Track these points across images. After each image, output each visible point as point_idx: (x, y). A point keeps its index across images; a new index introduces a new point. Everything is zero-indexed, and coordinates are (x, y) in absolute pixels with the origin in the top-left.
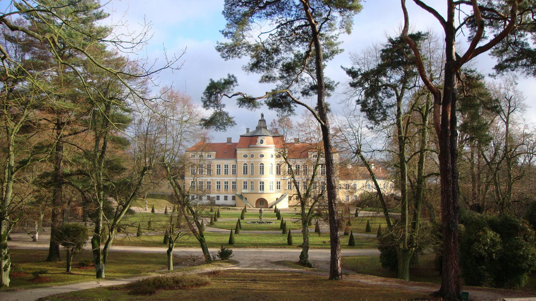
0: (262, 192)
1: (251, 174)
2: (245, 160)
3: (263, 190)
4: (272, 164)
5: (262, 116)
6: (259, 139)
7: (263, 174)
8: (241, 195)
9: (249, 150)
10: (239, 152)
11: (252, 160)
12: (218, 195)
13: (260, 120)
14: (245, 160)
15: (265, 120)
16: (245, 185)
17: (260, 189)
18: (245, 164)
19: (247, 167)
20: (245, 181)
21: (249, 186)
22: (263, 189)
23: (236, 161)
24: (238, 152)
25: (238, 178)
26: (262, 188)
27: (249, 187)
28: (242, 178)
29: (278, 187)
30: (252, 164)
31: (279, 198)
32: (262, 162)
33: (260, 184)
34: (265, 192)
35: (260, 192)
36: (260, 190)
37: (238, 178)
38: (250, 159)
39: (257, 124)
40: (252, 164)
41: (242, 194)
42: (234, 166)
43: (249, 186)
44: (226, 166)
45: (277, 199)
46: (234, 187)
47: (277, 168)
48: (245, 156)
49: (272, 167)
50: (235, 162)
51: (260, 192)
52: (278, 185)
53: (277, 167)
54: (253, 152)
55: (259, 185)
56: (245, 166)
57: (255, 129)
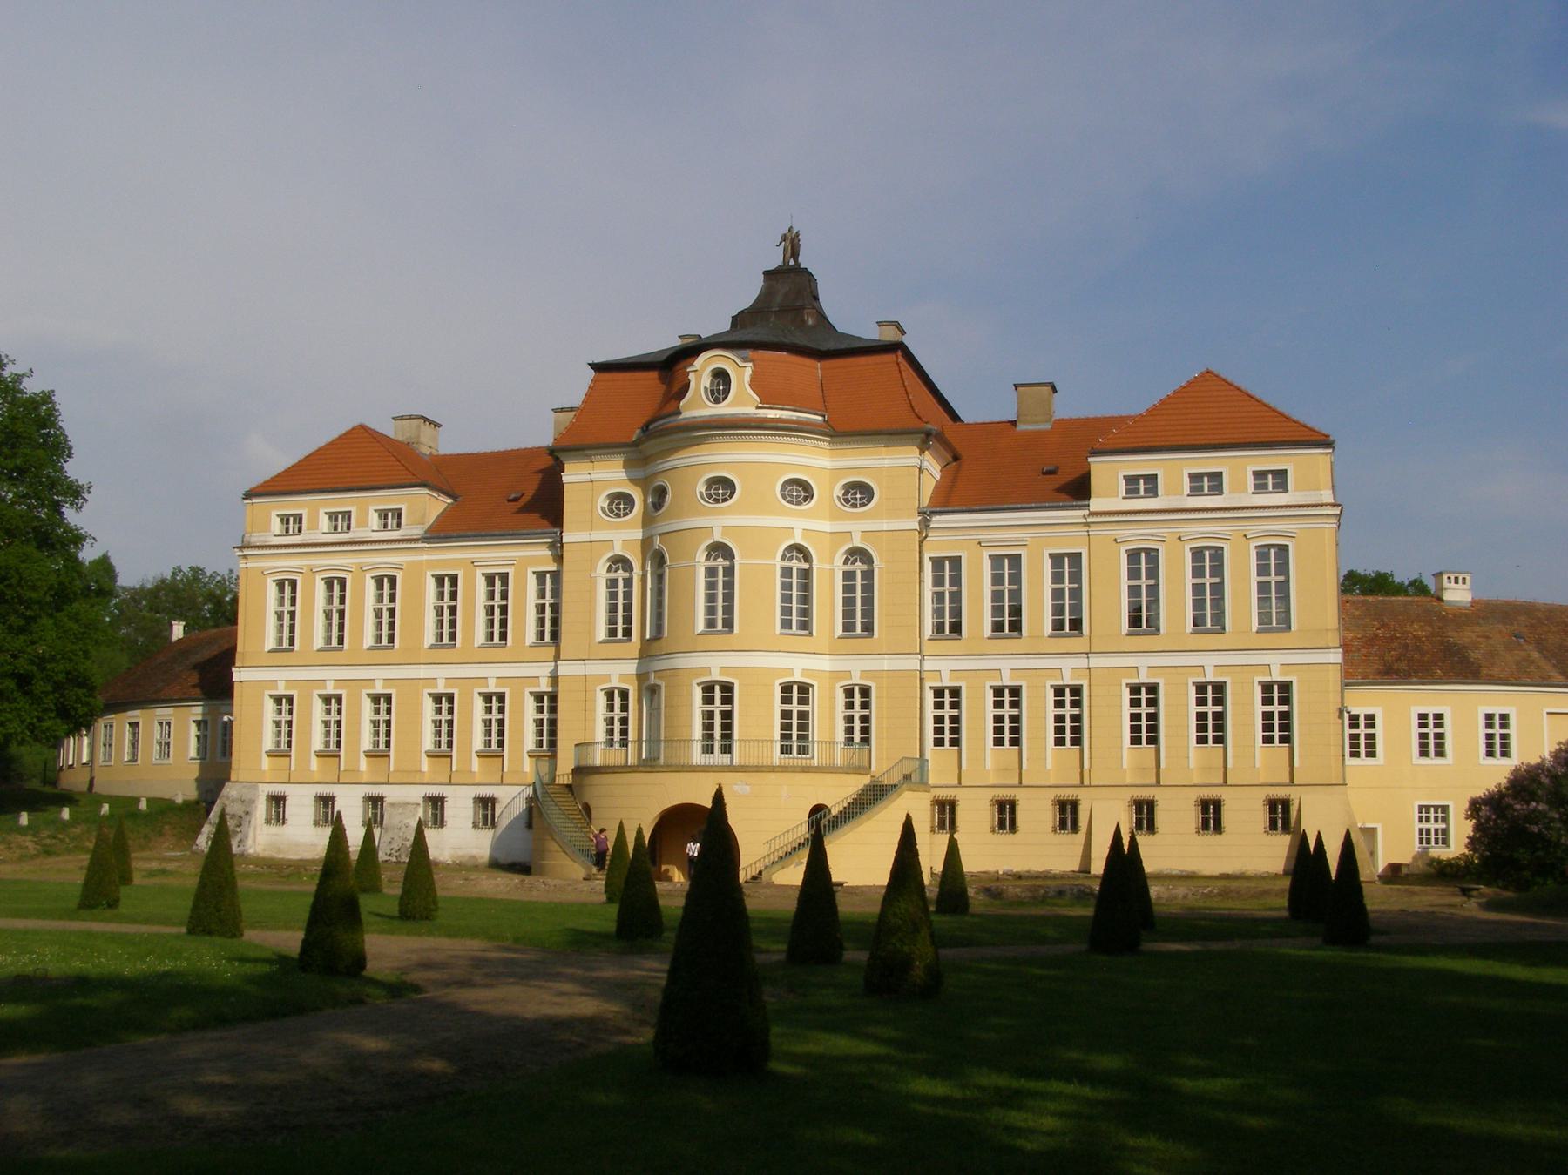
0: (718, 758)
3: (727, 749)
4: (800, 551)
5: (792, 244)
6: (701, 370)
10: (574, 475)
12: (434, 791)
17: (709, 737)
19: (628, 583)
20: (615, 683)
22: (727, 735)
24: (565, 478)
25: (564, 669)
34: (738, 756)
36: (709, 749)
37: (564, 669)
40: (659, 560)
42: (553, 581)
44: (497, 582)
48: (621, 503)
52: (857, 712)
57: (728, 327)
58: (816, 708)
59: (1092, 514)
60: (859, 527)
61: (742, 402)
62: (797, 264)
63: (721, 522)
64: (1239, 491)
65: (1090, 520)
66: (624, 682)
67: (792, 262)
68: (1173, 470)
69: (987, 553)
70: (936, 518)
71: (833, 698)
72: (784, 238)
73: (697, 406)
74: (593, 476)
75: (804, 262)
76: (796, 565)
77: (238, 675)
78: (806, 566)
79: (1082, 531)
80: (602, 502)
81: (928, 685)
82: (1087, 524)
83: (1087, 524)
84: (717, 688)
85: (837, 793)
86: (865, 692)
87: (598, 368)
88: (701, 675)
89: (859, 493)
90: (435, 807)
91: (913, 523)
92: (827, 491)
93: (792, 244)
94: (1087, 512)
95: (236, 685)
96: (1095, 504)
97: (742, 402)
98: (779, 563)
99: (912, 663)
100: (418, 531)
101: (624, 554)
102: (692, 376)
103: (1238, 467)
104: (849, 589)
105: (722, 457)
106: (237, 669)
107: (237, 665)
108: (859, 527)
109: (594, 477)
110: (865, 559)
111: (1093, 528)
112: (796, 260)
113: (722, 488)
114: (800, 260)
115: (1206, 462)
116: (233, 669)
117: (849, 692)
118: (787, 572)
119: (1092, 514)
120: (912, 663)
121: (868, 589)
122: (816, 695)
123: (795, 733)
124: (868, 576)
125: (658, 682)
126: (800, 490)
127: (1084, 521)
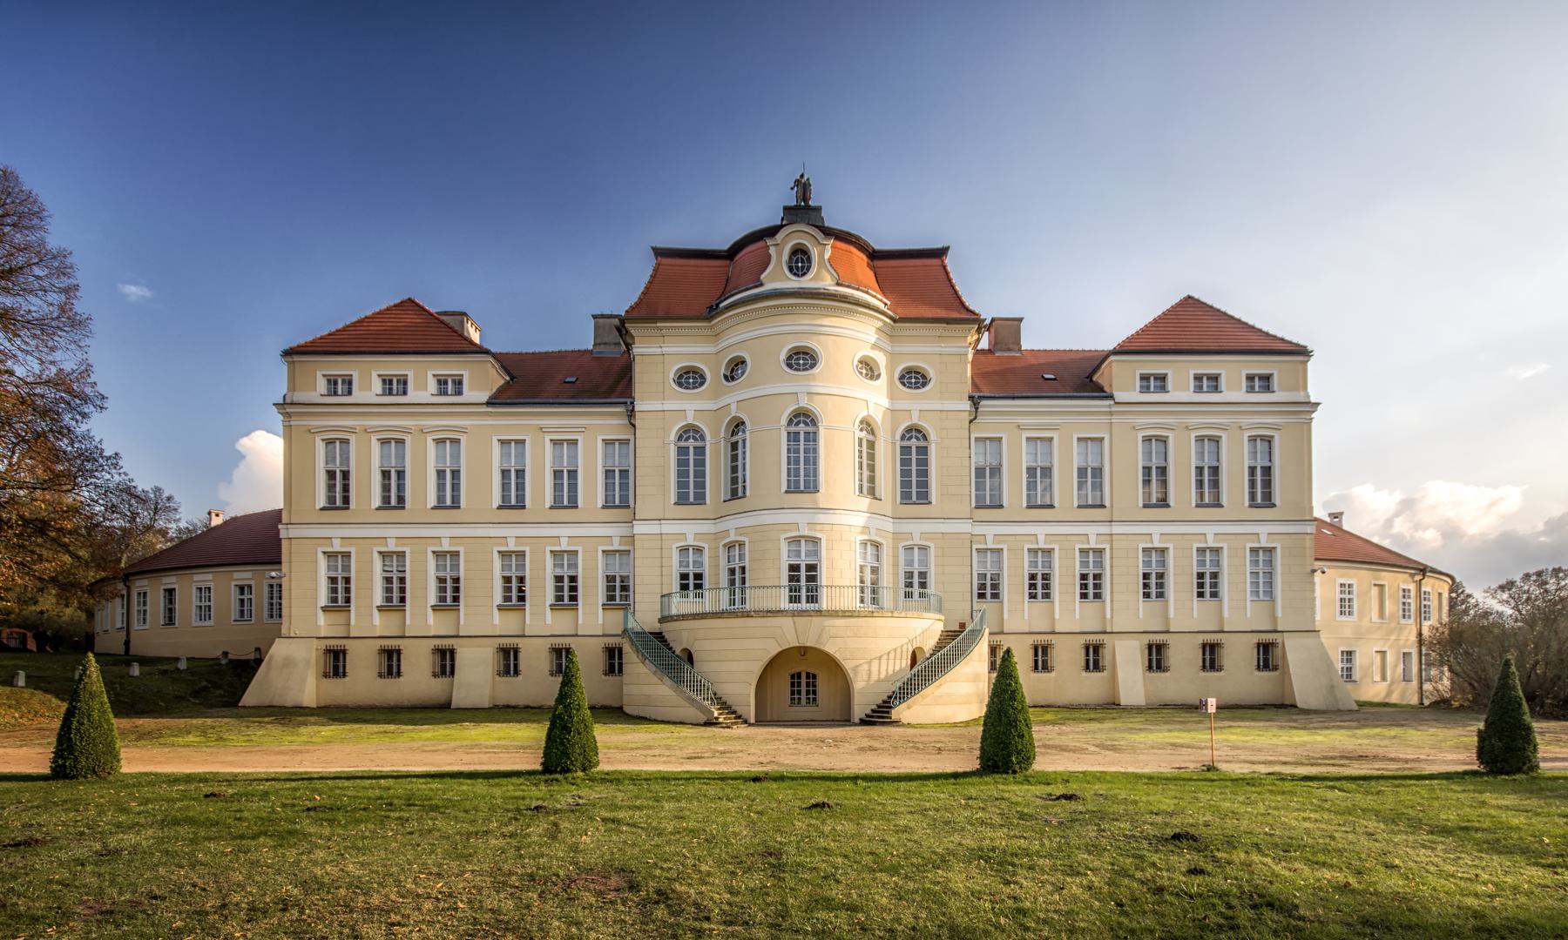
1: (724, 492)
2: (691, 407)
3: (812, 599)
7: (812, 487)
8: (659, 636)
19: (700, 451)
23: (631, 414)
25: (639, 528)
28: (668, 528)
32: (804, 402)
36: (794, 599)
38: (717, 395)
41: (669, 629)
46: (619, 591)
47: (905, 462)
48: (690, 378)
49: (871, 445)
53: (905, 450)
56: (691, 443)
59: (1116, 403)
64: (1234, 391)
65: (1113, 409)
66: (699, 540)
68: (1181, 372)
69: (1025, 435)
70: (984, 402)
74: (664, 349)
77: (283, 534)
79: (1105, 419)
80: (672, 375)
81: (975, 547)
82: (1111, 413)
83: (1111, 413)
88: (785, 531)
90: (390, 658)
91: (967, 405)
94: (1112, 402)
95: (283, 541)
96: (1120, 396)
99: (966, 527)
100: (484, 396)
101: (695, 423)
103: (1233, 371)
106: (284, 526)
107: (284, 521)
108: (918, 406)
110: (920, 436)
111: (1115, 419)
115: (1207, 365)
116: (280, 526)
118: (860, 440)
119: (1116, 403)
120: (966, 527)
121: (923, 462)
124: (923, 451)
127: (1108, 410)
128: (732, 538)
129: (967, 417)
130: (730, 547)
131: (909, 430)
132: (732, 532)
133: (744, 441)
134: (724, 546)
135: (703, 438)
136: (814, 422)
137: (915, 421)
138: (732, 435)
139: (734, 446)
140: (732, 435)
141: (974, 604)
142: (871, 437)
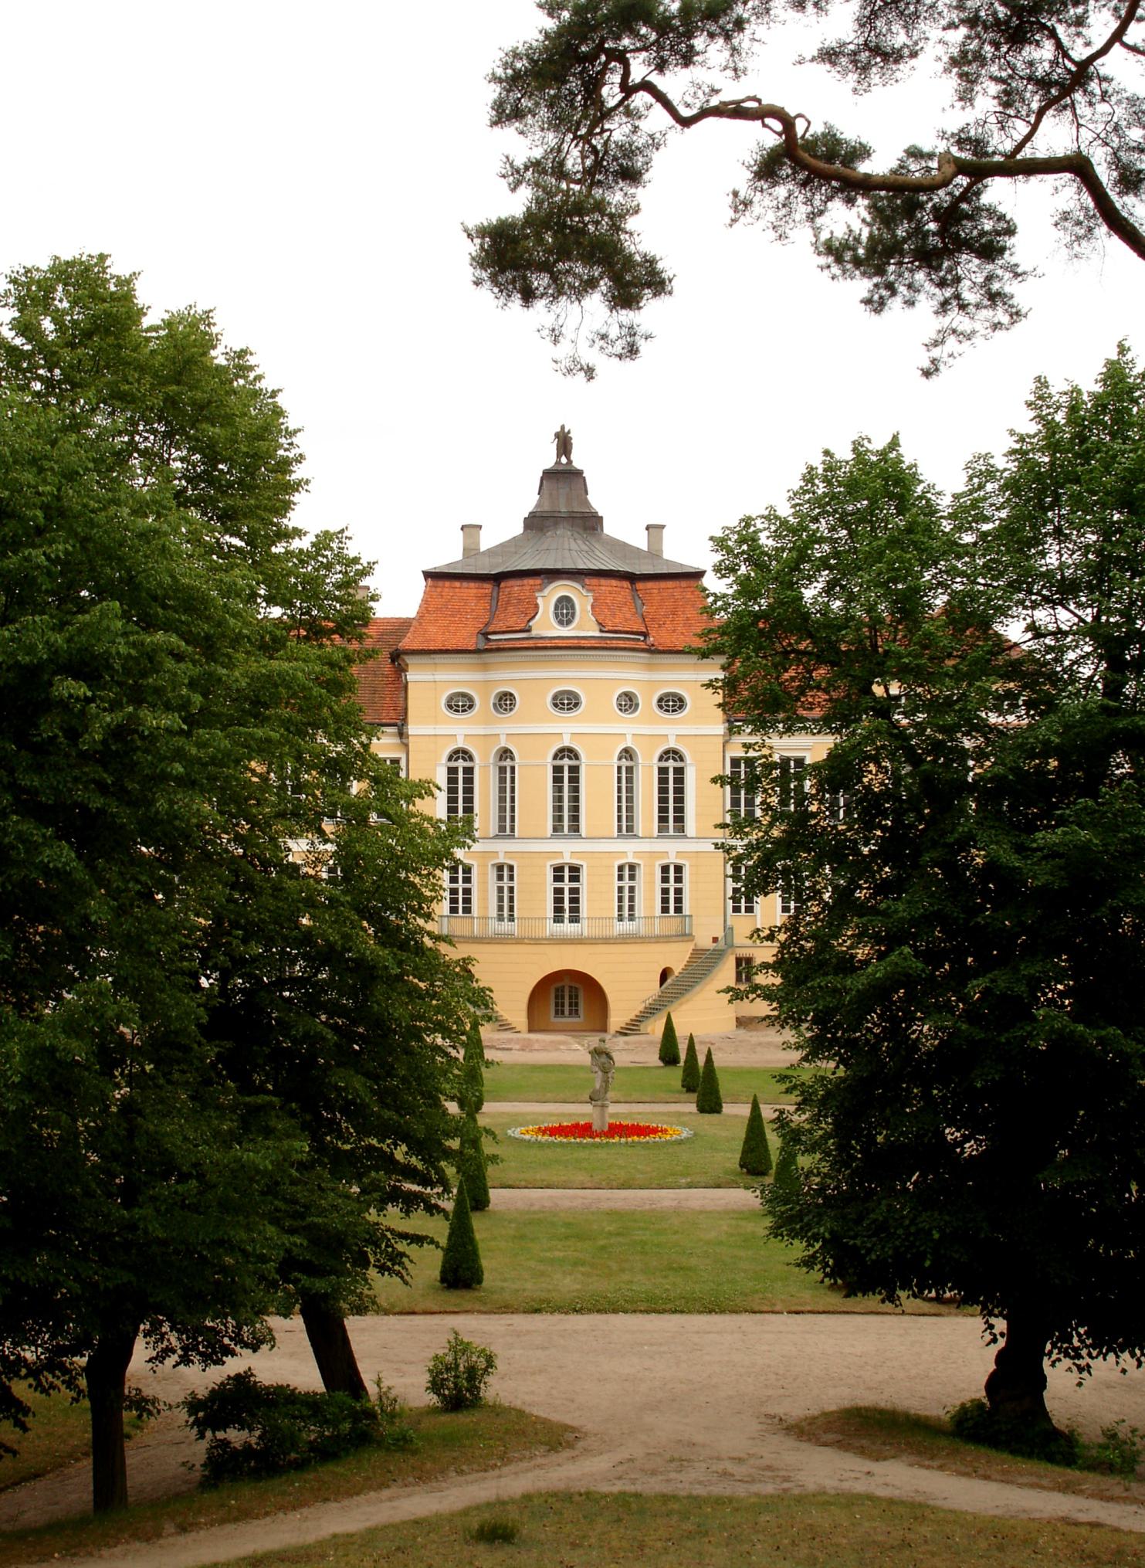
0: (567, 928)
2: (461, 731)
3: (575, 919)
4: (627, 754)
5: (564, 443)
6: (550, 595)
9: (485, 667)
11: (505, 729)
13: (548, 475)
14: (461, 731)
15: (579, 473)
16: (460, 885)
17: (559, 910)
18: (461, 754)
21: (484, 891)
23: (402, 734)
24: (411, 676)
26: (567, 905)
27: (484, 899)
29: (672, 901)
30: (506, 754)
31: (677, 970)
33: (558, 878)
35: (552, 928)
36: (558, 919)
39: (528, 500)
40: (506, 754)
43: (484, 891)
45: (665, 975)
48: (460, 704)
49: (630, 770)
50: (396, 740)
51: (552, 928)
52: (672, 885)
54: (509, 675)
55: (550, 885)
56: (461, 764)
58: (640, 884)
60: (672, 731)
61: (585, 626)
62: (570, 462)
63: (566, 729)
67: (564, 460)
71: (653, 874)
72: (557, 435)
73: (545, 625)
75: (578, 460)
76: (625, 763)
78: (629, 763)
80: (443, 701)
84: (567, 870)
85: (677, 957)
86: (679, 869)
87: (428, 575)
89: (672, 703)
92: (647, 701)
93: (564, 443)
97: (585, 626)
98: (615, 762)
102: (540, 601)
104: (663, 781)
105: (568, 675)
108: (672, 731)
109: (438, 678)
112: (568, 458)
113: (566, 702)
114: (573, 457)
117: (665, 869)
118: (619, 768)
122: (640, 873)
123: (626, 906)
125: (511, 862)
126: (628, 702)
128: (501, 860)
129: (721, 740)
130: (500, 868)
131: (667, 752)
132: (501, 855)
133: (513, 769)
134: (493, 865)
135: (471, 759)
136: (577, 757)
137: (672, 744)
138: (500, 760)
139: (502, 770)
140: (500, 760)
141: (728, 917)
142: (629, 763)
